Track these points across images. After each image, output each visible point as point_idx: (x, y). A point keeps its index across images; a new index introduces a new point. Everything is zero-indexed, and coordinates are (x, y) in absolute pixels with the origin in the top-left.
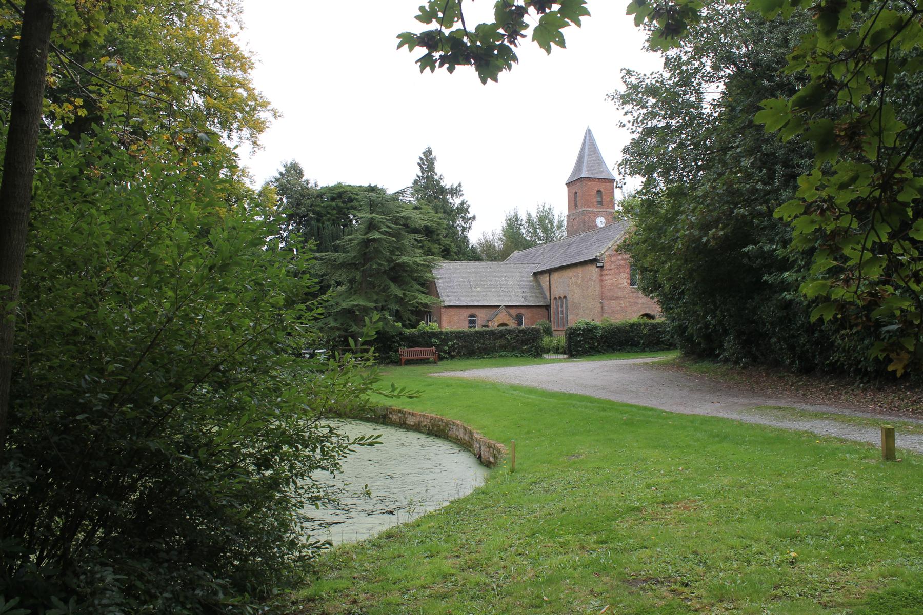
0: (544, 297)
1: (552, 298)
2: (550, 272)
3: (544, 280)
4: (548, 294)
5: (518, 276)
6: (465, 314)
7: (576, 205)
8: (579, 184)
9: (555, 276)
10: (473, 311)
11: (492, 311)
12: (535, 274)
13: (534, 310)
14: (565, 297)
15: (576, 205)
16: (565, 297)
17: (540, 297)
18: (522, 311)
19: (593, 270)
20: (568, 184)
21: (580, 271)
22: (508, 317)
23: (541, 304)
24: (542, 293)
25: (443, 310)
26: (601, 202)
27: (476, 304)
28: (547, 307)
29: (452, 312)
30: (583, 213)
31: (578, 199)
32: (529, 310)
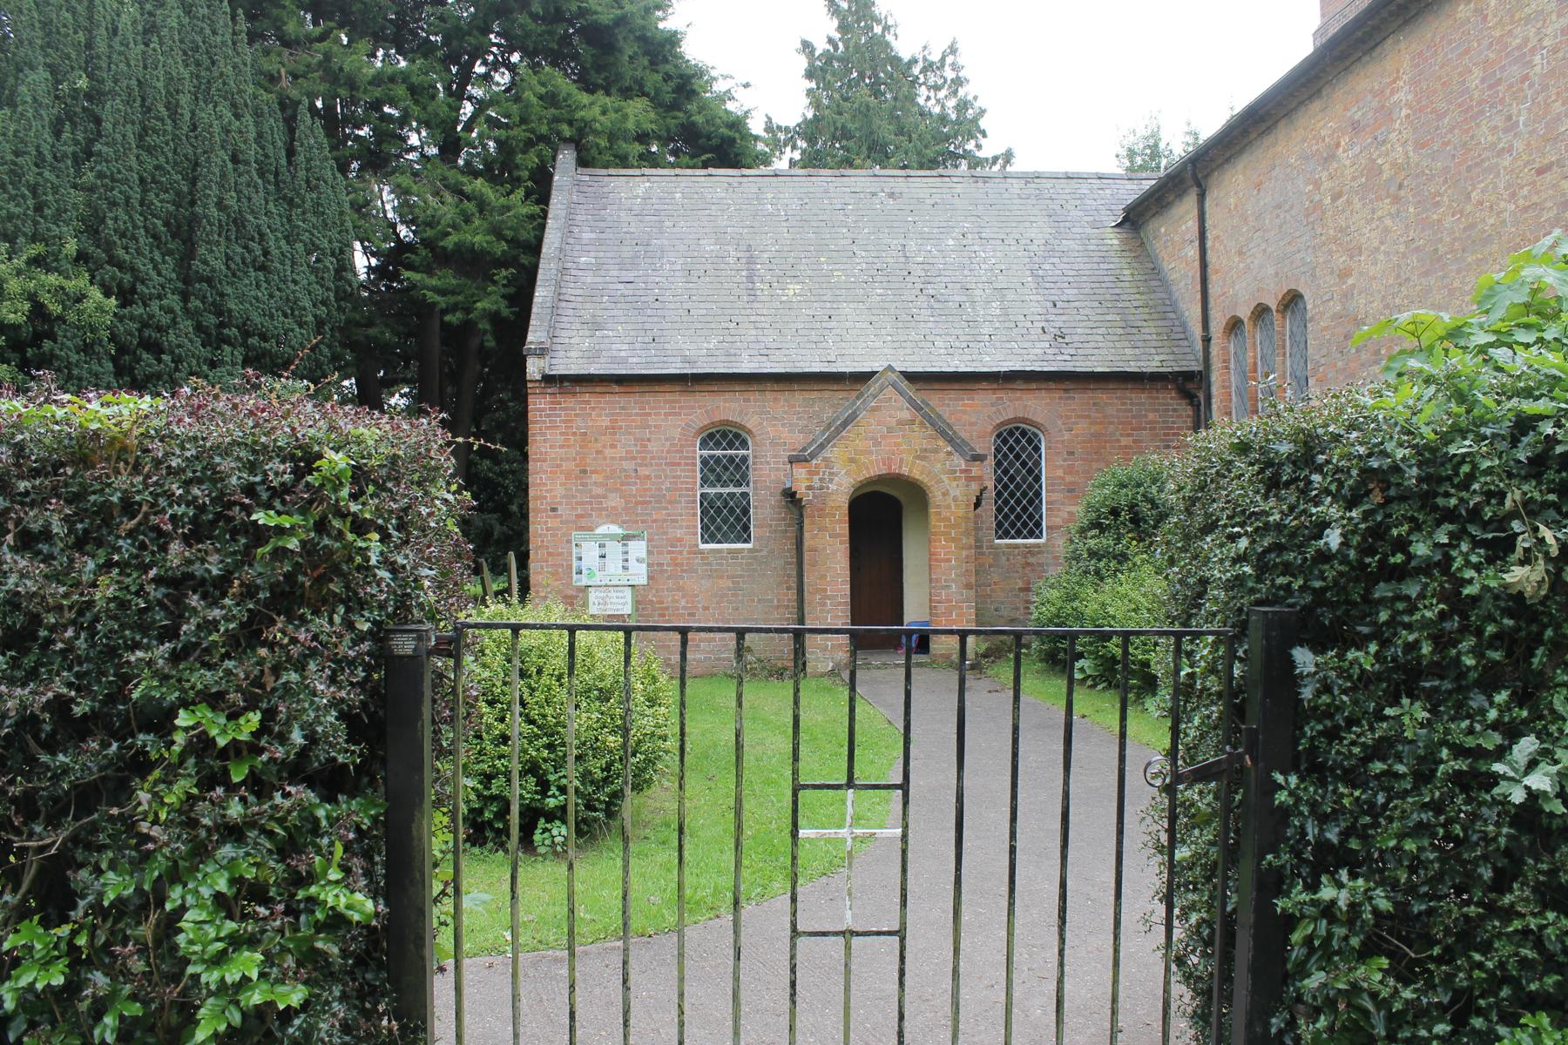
0: (1174, 331)
3: (1180, 221)
4: (1193, 312)
5: (1038, 232)
6: (675, 425)
11: (827, 405)
13: (1111, 402)
14: (1292, 301)
16: (1292, 301)
17: (1150, 329)
18: (1034, 406)
22: (920, 437)
23: (1152, 363)
24: (1166, 310)
25: (538, 405)
27: (746, 367)
28: (1189, 387)
29: (598, 411)
32: (1080, 400)
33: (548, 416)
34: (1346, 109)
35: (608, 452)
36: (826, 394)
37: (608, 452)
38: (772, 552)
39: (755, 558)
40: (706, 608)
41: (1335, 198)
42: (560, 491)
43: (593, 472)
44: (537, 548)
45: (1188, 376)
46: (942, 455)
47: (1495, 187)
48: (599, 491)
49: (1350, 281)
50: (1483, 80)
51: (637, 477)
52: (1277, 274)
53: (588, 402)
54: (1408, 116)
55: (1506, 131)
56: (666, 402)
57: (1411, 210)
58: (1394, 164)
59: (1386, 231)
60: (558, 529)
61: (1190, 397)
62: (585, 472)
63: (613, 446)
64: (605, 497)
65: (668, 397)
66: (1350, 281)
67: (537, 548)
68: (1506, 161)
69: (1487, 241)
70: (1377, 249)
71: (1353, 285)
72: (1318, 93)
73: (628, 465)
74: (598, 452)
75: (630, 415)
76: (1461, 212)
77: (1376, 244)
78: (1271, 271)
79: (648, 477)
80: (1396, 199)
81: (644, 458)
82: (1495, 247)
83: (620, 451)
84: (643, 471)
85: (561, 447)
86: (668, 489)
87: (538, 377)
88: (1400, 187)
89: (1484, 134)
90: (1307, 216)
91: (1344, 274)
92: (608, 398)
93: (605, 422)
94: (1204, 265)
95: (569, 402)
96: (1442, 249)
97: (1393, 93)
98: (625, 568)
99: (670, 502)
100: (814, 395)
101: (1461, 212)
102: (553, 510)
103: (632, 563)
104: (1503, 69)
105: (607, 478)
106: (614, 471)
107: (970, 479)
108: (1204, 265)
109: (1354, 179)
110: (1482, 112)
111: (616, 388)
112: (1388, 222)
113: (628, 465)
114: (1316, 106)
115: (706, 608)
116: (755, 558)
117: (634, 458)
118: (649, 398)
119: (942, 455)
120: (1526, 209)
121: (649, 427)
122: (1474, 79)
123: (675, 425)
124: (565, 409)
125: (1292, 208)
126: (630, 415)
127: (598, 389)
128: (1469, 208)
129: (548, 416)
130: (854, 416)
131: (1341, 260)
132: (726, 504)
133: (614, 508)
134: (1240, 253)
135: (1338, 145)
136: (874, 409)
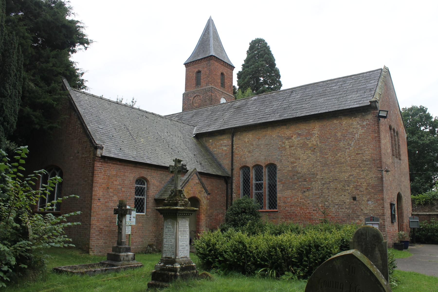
1: (237, 166)
2: (233, 132)
7: (198, 83)
8: (204, 63)
9: (248, 137)
10: (144, 173)
12: (198, 136)
15: (198, 83)
19: (357, 126)
20: (186, 64)
21: (316, 128)
22: (199, 187)
25: (98, 165)
26: (223, 85)
30: (211, 90)
31: (202, 75)
33: (100, 169)
34: (296, 130)
35: (115, 182)
36: (165, 172)
37: (115, 182)
38: (151, 216)
39: (147, 217)
40: (136, 232)
41: (290, 147)
42: (101, 193)
43: (111, 188)
44: (94, 212)
45: (228, 177)
46: (203, 193)
47: (344, 154)
48: (111, 194)
49: (295, 164)
50: (341, 135)
51: (121, 191)
52: (265, 159)
53: (111, 166)
54: (317, 136)
55: (348, 145)
56: (130, 169)
57: (318, 154)
58: (313, 144)
59: (309, 156)
60: (100, 206)
61: (227, 183)
62: (108, 188)
63: (116, 181)
64: (113, 196)
65: (131, 168)
66: (295, 164)
67: (94, 212)
68: (348, 150)
69: (343, 163)
70: (306, 160)
71: (297, 166)
72: (285, 125)
73: (119, 187)
74: (112, 182)
75: (121, 172)
76: (335, 157)
77: (306, 158)
78: (263, 158)
79: (124, 191)
80: (313, 151)
81: (123, 185)
82: (344, 165)
83: (117, 183)
84: (123, 190)
85: (103, 179)
86: (129, 196)
87: (100, 156)
88: (315, 149)
89: (341, 144)
90: (279, 149)
91: (293, 163)
92: (116, 166)
93: (114, 173)
94: (232, 152)
95: (106, 165)
96: (328, 163)
97: (313, 131)
98: (130, 220)
99: (129, 200)
100: (162, 172)
101: (335, 157)
102: (99, 199)
103: (132, 218)
104: (347, 135)
105: (114, 190)
106: (116, 189)
107: (208, 199)
108: (232, 152)
109: (298, 144)
110: (341, 141)
111: (119, 163)
112: (310, 155)
113: (119, 187)
114: (285, 127)
115: (136, 232)
116: (147, 217)
117: (121, 185)
118: (126, 167)
119: (203, 193)
120: (353, 160)
121: (125, 176)
122: (339, 134)
123: (131, 176)
124: (104, 167)
125: (273, 146)
126: (121, 172)
127: (114, 162)
128: (337, 157)
129: (100, 169)
130: (189, 180)
131: (292, 160)
132: (139, 201)
133: (115, 200)
134: (249, 152)
135: (292, 137)
136: (192, 179)
